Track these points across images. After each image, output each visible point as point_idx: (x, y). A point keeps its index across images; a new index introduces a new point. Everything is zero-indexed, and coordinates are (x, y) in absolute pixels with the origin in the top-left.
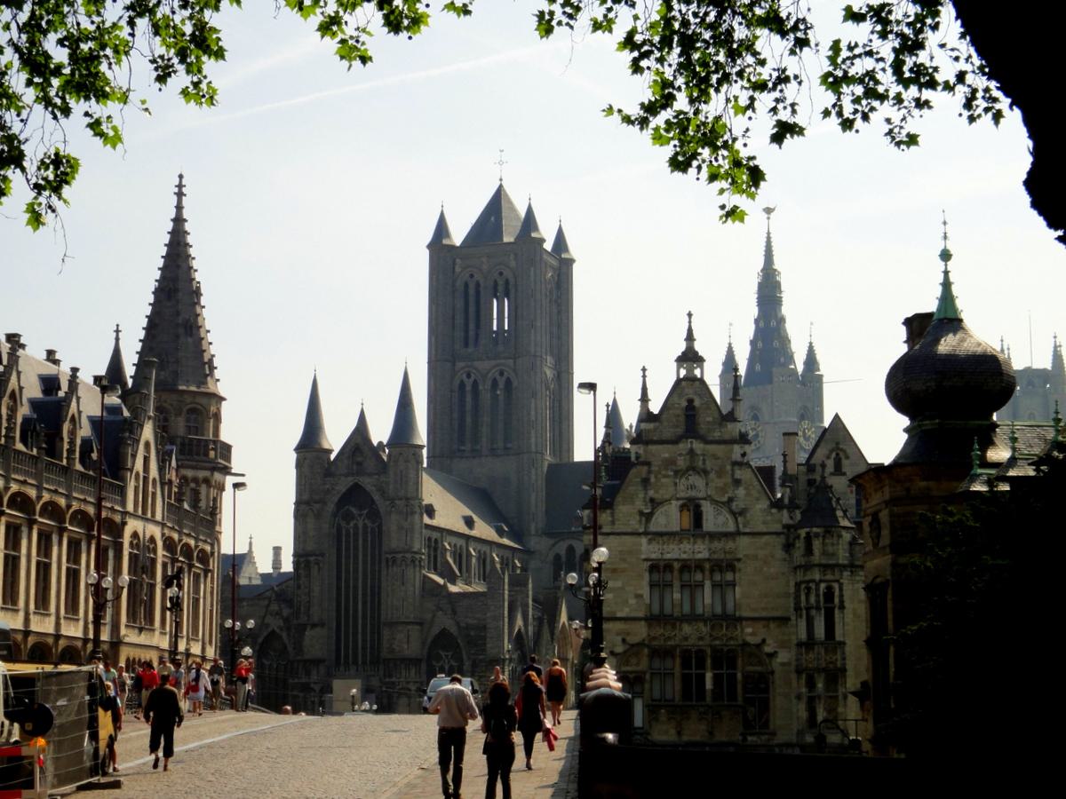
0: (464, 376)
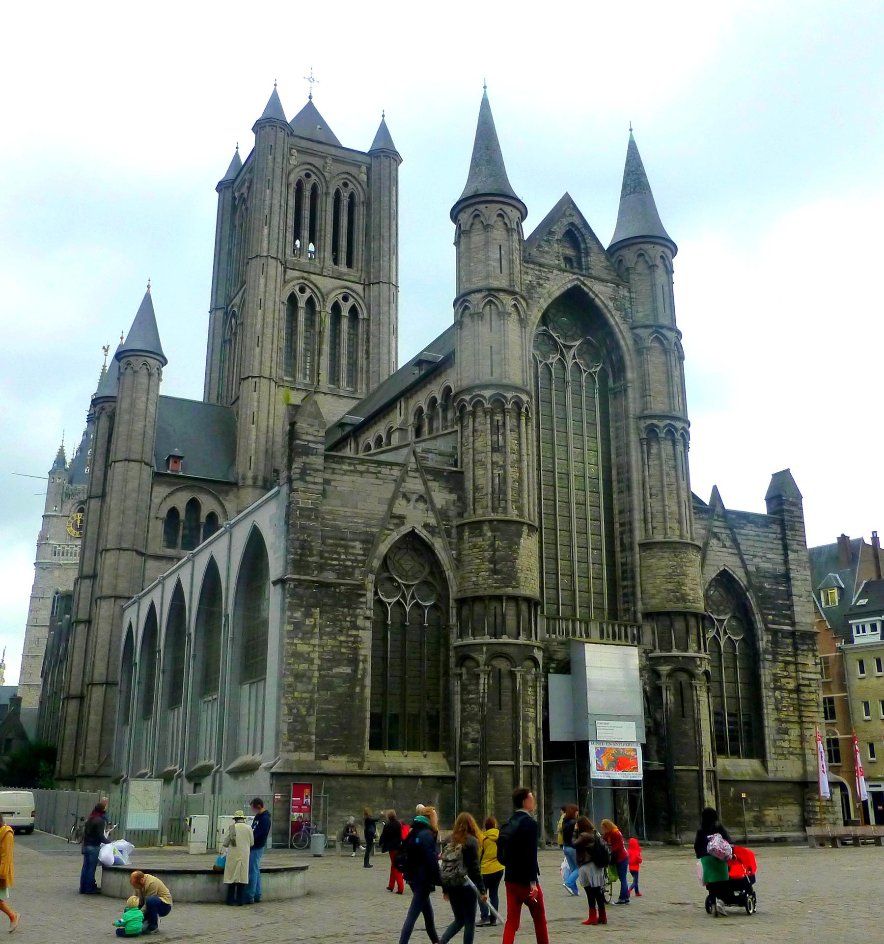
0: (297, 288)
